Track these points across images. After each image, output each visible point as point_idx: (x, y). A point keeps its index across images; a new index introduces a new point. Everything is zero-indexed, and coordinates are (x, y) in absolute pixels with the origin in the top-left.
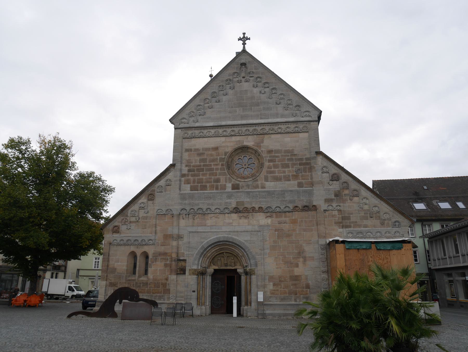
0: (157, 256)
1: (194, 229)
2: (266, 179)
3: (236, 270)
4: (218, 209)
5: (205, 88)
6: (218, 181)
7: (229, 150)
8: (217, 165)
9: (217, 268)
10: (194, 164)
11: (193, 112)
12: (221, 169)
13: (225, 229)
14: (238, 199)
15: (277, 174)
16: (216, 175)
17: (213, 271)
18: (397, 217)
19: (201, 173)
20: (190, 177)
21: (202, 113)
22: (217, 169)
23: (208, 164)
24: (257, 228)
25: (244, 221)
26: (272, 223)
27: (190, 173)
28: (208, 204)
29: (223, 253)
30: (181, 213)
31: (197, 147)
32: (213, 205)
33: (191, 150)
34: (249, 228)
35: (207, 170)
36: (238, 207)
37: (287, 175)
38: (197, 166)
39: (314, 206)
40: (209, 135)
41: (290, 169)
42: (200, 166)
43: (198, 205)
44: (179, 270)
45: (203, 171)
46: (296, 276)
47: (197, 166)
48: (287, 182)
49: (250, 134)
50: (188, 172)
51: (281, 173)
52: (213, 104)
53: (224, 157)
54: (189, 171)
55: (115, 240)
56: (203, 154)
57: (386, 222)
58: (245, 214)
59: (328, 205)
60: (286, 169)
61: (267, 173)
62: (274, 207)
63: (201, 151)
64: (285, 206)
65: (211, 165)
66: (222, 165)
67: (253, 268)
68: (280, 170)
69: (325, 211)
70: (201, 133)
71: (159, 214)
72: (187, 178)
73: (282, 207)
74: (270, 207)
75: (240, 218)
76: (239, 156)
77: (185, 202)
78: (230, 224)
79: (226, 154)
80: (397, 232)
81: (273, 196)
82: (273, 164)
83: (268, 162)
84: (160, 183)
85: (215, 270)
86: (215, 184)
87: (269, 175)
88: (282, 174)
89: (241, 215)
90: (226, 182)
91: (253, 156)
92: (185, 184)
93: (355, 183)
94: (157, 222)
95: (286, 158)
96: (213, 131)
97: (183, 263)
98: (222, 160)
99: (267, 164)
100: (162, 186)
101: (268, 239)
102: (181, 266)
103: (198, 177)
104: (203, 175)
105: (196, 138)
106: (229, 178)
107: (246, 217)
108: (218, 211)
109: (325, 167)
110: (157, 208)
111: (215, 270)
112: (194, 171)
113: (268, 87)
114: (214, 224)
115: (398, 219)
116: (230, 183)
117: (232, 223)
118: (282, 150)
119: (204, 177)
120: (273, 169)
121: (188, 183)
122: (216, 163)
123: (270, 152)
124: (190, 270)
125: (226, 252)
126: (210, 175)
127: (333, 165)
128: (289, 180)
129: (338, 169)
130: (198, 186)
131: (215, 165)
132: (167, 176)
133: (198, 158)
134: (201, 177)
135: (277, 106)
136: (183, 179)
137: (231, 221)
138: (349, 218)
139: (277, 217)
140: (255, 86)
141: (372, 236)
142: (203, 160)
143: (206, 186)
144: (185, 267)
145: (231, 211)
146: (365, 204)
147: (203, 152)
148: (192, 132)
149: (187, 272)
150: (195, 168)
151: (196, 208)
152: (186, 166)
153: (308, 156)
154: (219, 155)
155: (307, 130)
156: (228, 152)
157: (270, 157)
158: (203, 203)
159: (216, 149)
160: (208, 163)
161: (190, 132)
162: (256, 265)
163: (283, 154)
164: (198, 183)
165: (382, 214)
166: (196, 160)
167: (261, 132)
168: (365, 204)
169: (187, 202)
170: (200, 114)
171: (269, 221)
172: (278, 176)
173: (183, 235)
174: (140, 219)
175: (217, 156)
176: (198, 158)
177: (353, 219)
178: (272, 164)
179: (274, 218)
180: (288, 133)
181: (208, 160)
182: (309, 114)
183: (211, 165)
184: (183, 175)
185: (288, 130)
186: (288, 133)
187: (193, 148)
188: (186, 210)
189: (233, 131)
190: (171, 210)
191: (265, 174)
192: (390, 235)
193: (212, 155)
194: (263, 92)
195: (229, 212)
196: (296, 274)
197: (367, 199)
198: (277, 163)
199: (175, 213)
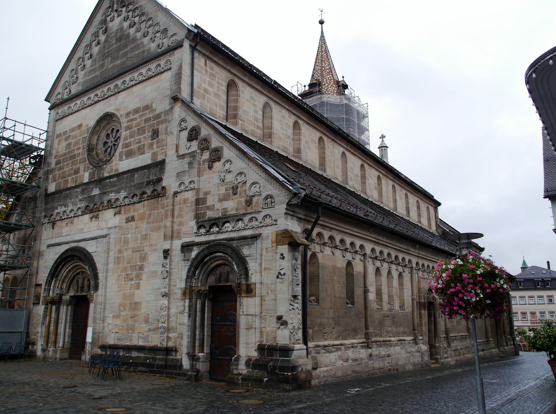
5: (79, 44)
6: (77, 171)
7: (92, 123)
16: (77, 164)
18: (269, 189)
24: (104, 232)
39: (164, 188)
46: (136, 303)
48: (141, 157)
49: (112, 94)
58: (95, 214)
59: (179, 183)
60: (142, 137)
64: (132, 194)
69: (176, 193)
80: (268, 217)
88: (137, 145)
89: (92, 215)
90: (84, 171)
93: (216, 137)
95: (144, 119)
106: (88, 164)
107: (97, 217)
115: (271, 192)
116: (87, 171)
118: (140, 108)
138: (204, 200)
139: (125, 214)
141: (230, 228)
142: (69, 145)
146: (229, 172)
159: (80, 126)
163: (141, 113)
168: (229, 172)
176: (64, 144)
177: (209, 202)
185: (150, 73)
191: (121, 150)
192: (257, 223)
196: (136, 300)
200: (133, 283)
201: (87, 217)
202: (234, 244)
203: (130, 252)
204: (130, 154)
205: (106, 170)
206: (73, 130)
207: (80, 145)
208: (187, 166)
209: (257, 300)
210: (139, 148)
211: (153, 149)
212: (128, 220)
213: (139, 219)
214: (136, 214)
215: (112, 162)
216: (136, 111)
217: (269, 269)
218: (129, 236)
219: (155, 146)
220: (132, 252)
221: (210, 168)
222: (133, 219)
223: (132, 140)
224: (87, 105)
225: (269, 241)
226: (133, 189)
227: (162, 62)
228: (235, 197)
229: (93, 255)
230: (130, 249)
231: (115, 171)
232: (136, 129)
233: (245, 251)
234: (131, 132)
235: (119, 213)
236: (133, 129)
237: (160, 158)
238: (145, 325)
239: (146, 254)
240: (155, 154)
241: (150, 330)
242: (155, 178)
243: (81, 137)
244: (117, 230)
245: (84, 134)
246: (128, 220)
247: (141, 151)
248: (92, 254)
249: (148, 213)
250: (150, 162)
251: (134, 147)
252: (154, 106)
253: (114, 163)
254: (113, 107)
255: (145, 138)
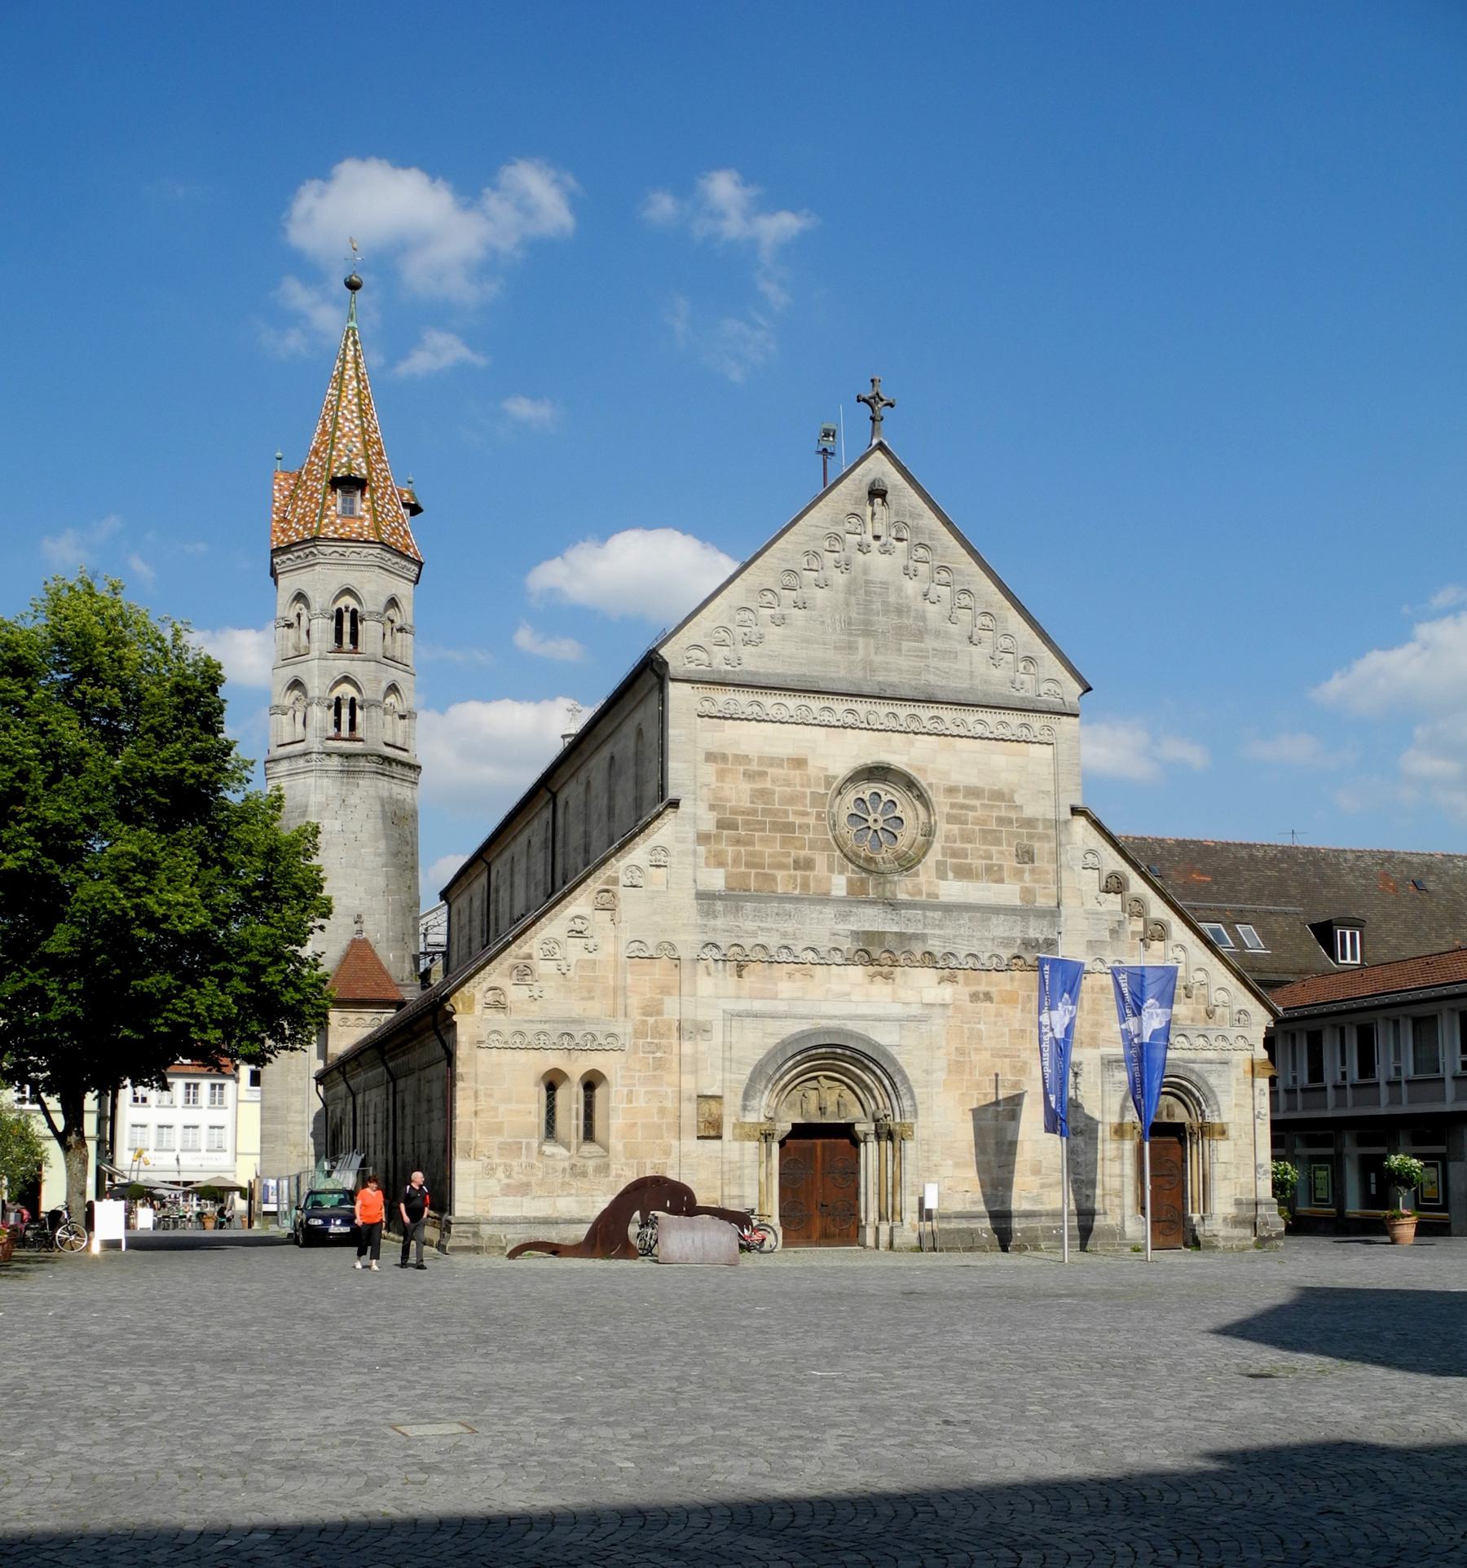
0: (635, 1086)
1: (744, 1005)
2: (942, 876)
3: (851, 1125)
4: (813, 949)
6: (808, 864)
7: (842, 769)
8: (805, 814)
9: (800, 1120)
10: (734, 803)
11: (726, 630)
12: (815, 828)
13: (829, 1008)
14: (867, 925)
15: (968, 861)
16: (802, 847)
17: (790, 1128)
19: (757, 834)
20: (723, 846)
21: (753, 638)
22: (805, 827)
23: (779, 810)
24: (915, 1010)
25: (881, 989)
26: (955, 1000)
27: (725, 832)
28: (784, 935)
29: (815, 1078)
30: (704, 956)
31: (743, 750)
32: (796, 939)
33: (724, 757)
34: (896, 1010)
35: (775, 827)
36: (870, 949)
37: (993, 865)
38: (743, 813)
40: (779, 717)
41: (1004, 847)
42: (754, 812)
43: (754, 934)
44: (702, 1125)
45: (763, 830)
47: (743, 813)
50: (718, 827)
51: (981, 857)
52: (786, 612)
53: (823, 791)
54: (722, 825)
55: (495, 1032)
56: (764, 774)
57: (1218, 1011)
58: (886, 969)
60: (994, 849)
61: (944, 854)
62: (962, 955)
63: (754, 767)
65: (786, 812)
66: (819, 816)
67: (908, 1121)
68: (978, 849)
70: (756, 708)
71: (632, 955)
72: (714, 846)
73: (984, 957)
74: (952, 954)
75: (873, 976)
76: (858, 792)
77: (713, 922)
78: (844, 996)
79: (829, 780)
81: (961, 922)
82: (959, 829)
83: (948, 823)
84: (631, 856)
85: (794, 1125)
86: (798, 873)
87: (949, 860)
88: (984, 862)
90: (831, 870)
91: (897, 794)
92: (707, 865)
94: (629, 981)
95: (995, 814)
96: (792, 702)
97: (713, 1103)
98: (817, 799)
99: (943, 828)
100: (638, 868)
101: (944, 1043)
102: (710, 1115)
103: (750, 848)
104: (762, 840)
105: (739, 719)
107: (887, 977)
108: (810, 956)
109: (1091, 851)
110: (627, 936)
111: (794, 1125)
112: (733, 826)
113: (947, 585)
114: (800, 994)
116: (841, 872)
117: (849, 994)
118: (983, 790)
119: (768, 851)
120: (958, 845)
121: (721, 864)
122: (801, 809)
123: (951, 790)
124: (735, 1125)
125: (826, 1077)
126: (785, 842)
127: (1110, 850)
128: (1001, 881)
129: (1122, 862)
130: (746, 875)
131: (796, 813)
132: (654, 837)
133: (746, 787)
134: (758, 847)
135: (973, 648)
136: (702, 849)
137: (846, 988)
139: (967, 984)
140: (912, 574)
142: (762, 794)
143: (773, 878)
144: (721, 1116)
145: (847, 959)
147: (761, 769)
148: (728, 697)
149: (727, 1132)
150: (740, 818)
151: (748, 943)
152: (712, 807)
153: (1051, 815)
154: (809, 786)
155: (1050, 738)
156: (835, 777)
157: (953, 806)
158: (769, 930)
159: (799, 763)
160: (777, 806)
161: (722, 698)
162: (915, 1114)
163: (986, 802)
164: (747, 865)
165: (1213, 988)
166: (739, 792)
167: (928, 726)
169: (720, 922)
170: (746, 638)
171: (946, 992)
172: (971, 864)
173: (711, 1022)
174: (572, 968)
175: (802, 786)
178: (955, 828)
179: (959, 986)
180: (1003, 740)
181: (777, 796)
182: (1058, 691)
183: (786, 812)
184: (703, 838)
186: (1003, 740)
187: (729, 752)
188: (717, 947)
189: (850, 711)
190: (671, 944)
191: (940, 858)
192: (1224, 1044)
193: (788, 783)
194: (932, 596)
195: (840, 961)
197: (1183, 948)
198: (969, 826)
199: (685, 953)
200: (1000, 1109)
201: (857, 973)
202: (1196, 1067)
203: (986, 1055)
204: (963, 873)
205: (903, 885)
206: (774, 761)
207: (806, 806)
208: (1107, 933)
209: (1231, 1143)
210: (989, 869)
211: (1022, 880)
212: (974, 997)
213: (1004, 1002)
214: (993, 990)
215: (917, 875)
216: (973, 792)
217: (1242, 1106)
218: (982, 1026)
219: (1027, 876)
220: (992, 1056)
221: (1147, 947)
222: (988, 997)
223: (968, 846)
224: (816, 722)
225: (1241, 1070)
226: (989, 943)
227: (1037, 722)
228: (1188, 1000)
229: (894, 1052)
230: (986, 1049)
231: (929, 895)
232: (977, 828)
233: (1213, 1080)
234: (963, 829)
235: (952, 980)
236: (969, 826)
237: (1044, 901)
238: (1034, 1178)
239: (1025, 1063)
240: (1027, 893)
241: (1043, 1186)
242: (1041, 938)
243: (808, 791)
244: (950, 1012)
245: (819, 785)
246: (974, 997)
247: (994, 874)
248: (889, 1049)
249: (1022, 993)
250: (1018, 902)
251: (978, 863)
252: (1018, 800)
253: (922, 879)
254: (905, 759)
255: (1001, 853)
